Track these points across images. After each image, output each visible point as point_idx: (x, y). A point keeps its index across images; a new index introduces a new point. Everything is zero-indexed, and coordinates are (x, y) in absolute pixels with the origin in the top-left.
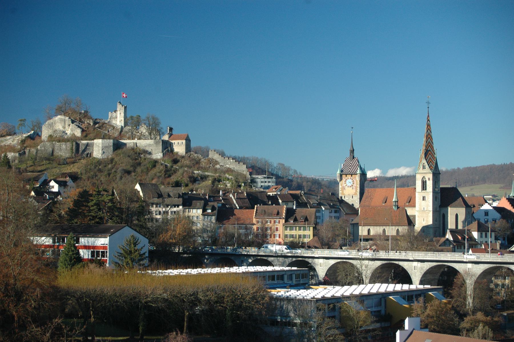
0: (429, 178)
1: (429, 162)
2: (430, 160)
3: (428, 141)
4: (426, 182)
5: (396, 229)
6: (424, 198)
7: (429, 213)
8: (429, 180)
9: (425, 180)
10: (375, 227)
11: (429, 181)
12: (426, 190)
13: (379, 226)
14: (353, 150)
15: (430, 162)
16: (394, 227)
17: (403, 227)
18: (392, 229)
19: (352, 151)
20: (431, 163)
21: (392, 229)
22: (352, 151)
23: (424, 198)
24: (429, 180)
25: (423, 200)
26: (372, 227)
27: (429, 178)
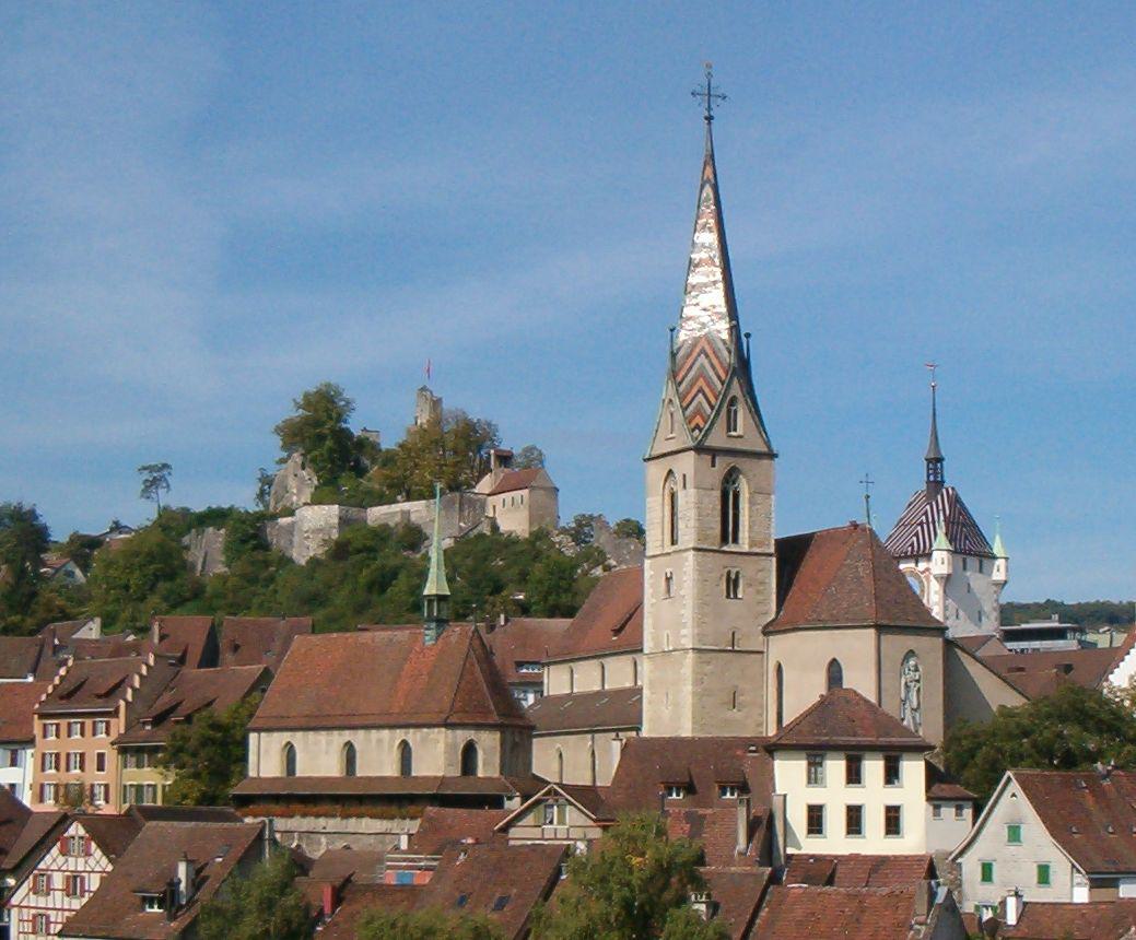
0: (684, 476)
2: (701, 382)
5: (398, 742)
10: (311, 734)
11: (684, 492)
14: (940, 460)
15: (701, 390)
16: (386, 733)
17: (425, 730)
18: (380, 741)
19: (935, 462)
20: (700, 395)
21: (380, 741)
22: (935, 462)
27: (684, 476)
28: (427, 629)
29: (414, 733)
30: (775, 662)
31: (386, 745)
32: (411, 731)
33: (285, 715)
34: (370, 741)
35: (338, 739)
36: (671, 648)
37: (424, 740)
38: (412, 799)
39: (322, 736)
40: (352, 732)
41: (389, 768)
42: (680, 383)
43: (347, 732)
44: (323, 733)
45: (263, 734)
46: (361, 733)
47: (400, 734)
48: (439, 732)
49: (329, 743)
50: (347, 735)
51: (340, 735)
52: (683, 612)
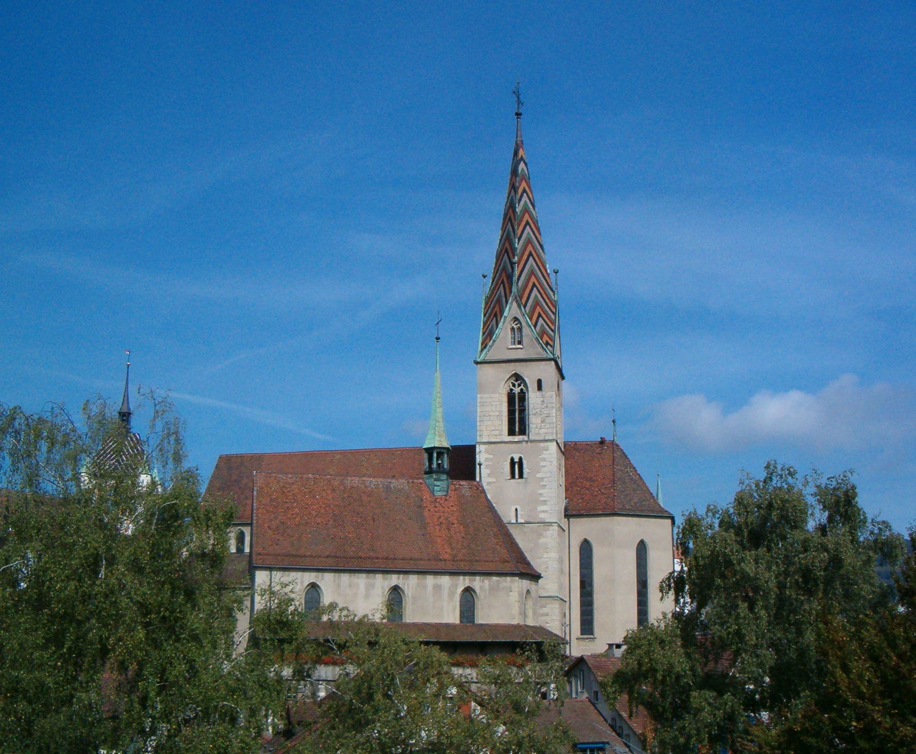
0: (539, 382)
1: (536, 315)
3: (524, 236)
4: (523, 397)
5: (460, 589)
6: (517, 468)
7: (540, 535)
8: (540, 387)
9: (517, 390)
10: (345, 578)
11: (539, 393)
12: (523, 432)
13: (368, 572)
16: (445, 580)
17: (495, 578)
18: (437, 588)
21: (437, 588)
23: (517, 468)
24: (540, 387)
25: (513, 476)
26: (329, 576)
27: (539, 382)
28: (436, 480)
29: (464, 580)
30: (581, 539)
31: (446, 592)
32: (478, 578)
33: (392, 556)
34: (425, 587)
35: (382, 584)
36: (520, 520)
37: (493, 589)
38: (483, 648)
39: (361, 580)
40: (421, 576)
41: (452, 616)
42: (525, 307)
43: (394, 577)
44: (364, 575)
45: (274, 573)
46: (413, 579)
47: (463, 582)
48: (512, 581)
49: (370, 587)
50: (394, 580)
51: (367, 578)
52: (540, 492)
